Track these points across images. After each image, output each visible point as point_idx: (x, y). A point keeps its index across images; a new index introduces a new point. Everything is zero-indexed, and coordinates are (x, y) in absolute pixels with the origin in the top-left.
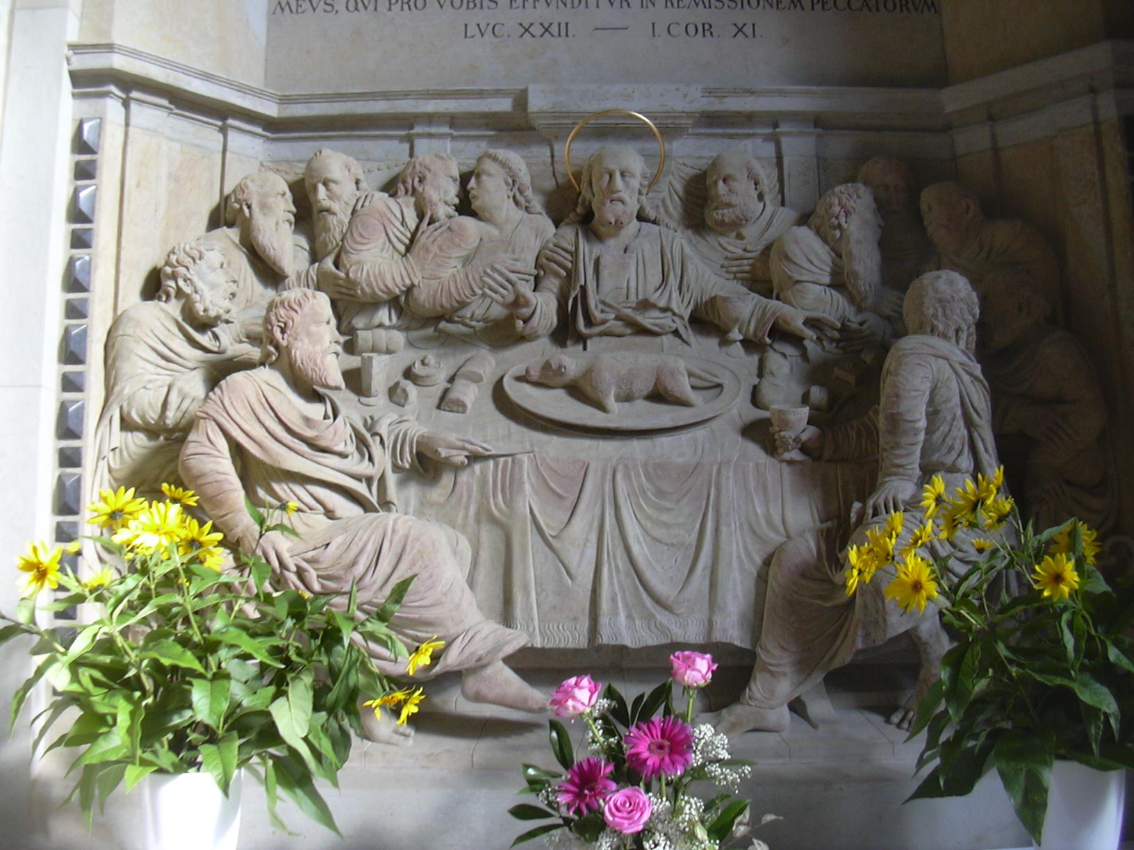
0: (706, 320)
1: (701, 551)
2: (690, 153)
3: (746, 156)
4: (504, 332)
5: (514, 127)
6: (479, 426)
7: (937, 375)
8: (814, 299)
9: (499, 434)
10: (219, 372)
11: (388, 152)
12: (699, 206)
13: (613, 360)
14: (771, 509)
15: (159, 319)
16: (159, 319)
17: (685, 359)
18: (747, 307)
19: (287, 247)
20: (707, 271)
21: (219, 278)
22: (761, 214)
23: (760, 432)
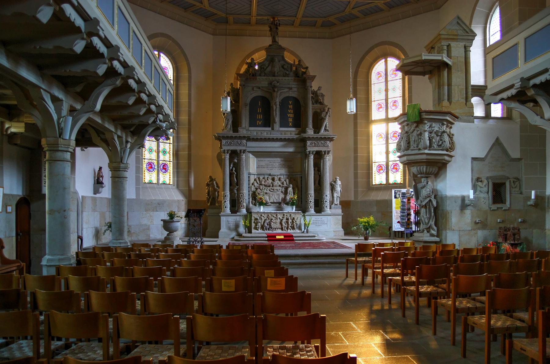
0: (280, 186)
1: (279, 198)
2: (279, 177)
3: (282, 177)
4: (269, 186)
5: (270, 175)
6: (268, 191)
7: (290, 189)
8: (285, 185)
9: (269, 192)
10: (257, 189)
11: (263, 176)
12: (280, 180)
13: (275, 188)
14: (282, 196)
15: (253, 186)
16: (253, 186)
17: (278, 188)
18: (282, 185)
19: (258, 182)
20: (280, 183)
21: (256, 184)
22: (283, 180)
23: (282, 192)
